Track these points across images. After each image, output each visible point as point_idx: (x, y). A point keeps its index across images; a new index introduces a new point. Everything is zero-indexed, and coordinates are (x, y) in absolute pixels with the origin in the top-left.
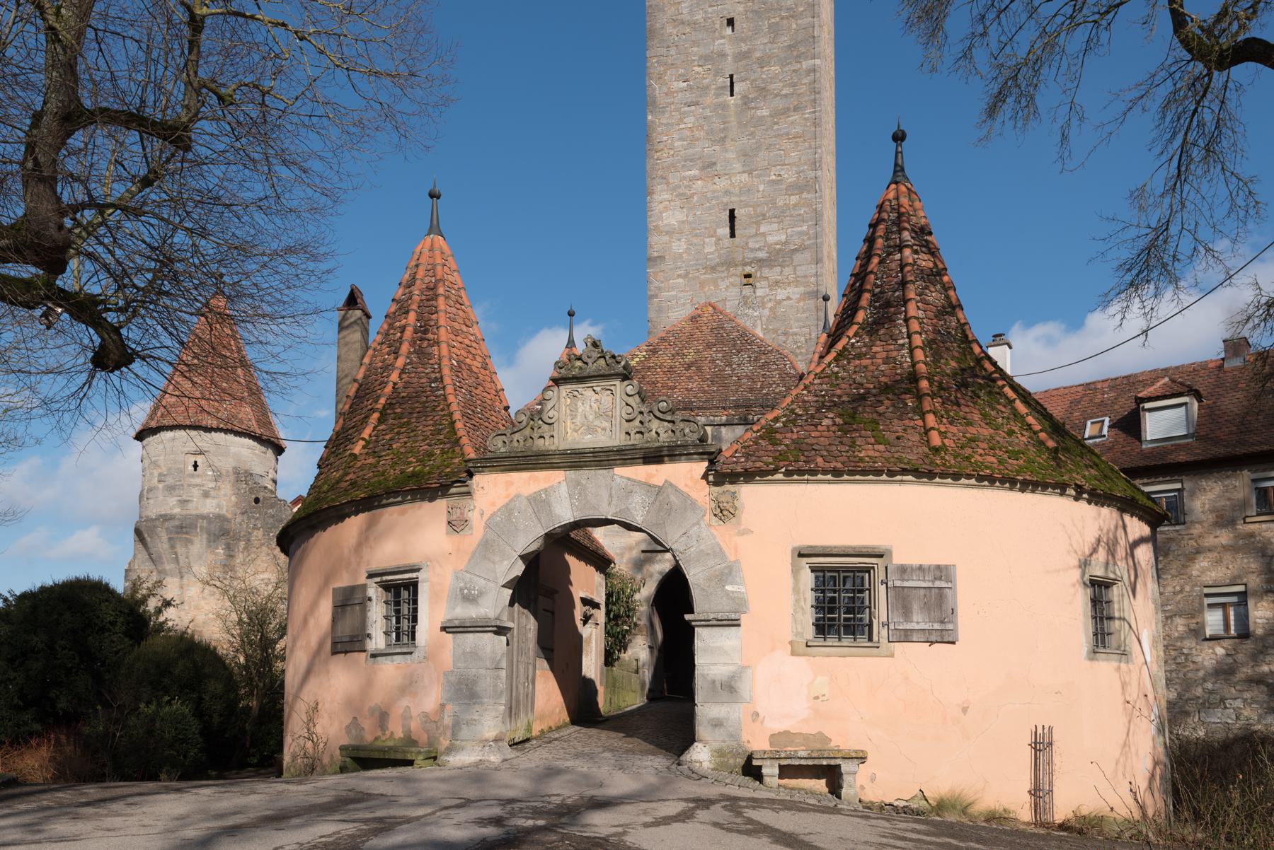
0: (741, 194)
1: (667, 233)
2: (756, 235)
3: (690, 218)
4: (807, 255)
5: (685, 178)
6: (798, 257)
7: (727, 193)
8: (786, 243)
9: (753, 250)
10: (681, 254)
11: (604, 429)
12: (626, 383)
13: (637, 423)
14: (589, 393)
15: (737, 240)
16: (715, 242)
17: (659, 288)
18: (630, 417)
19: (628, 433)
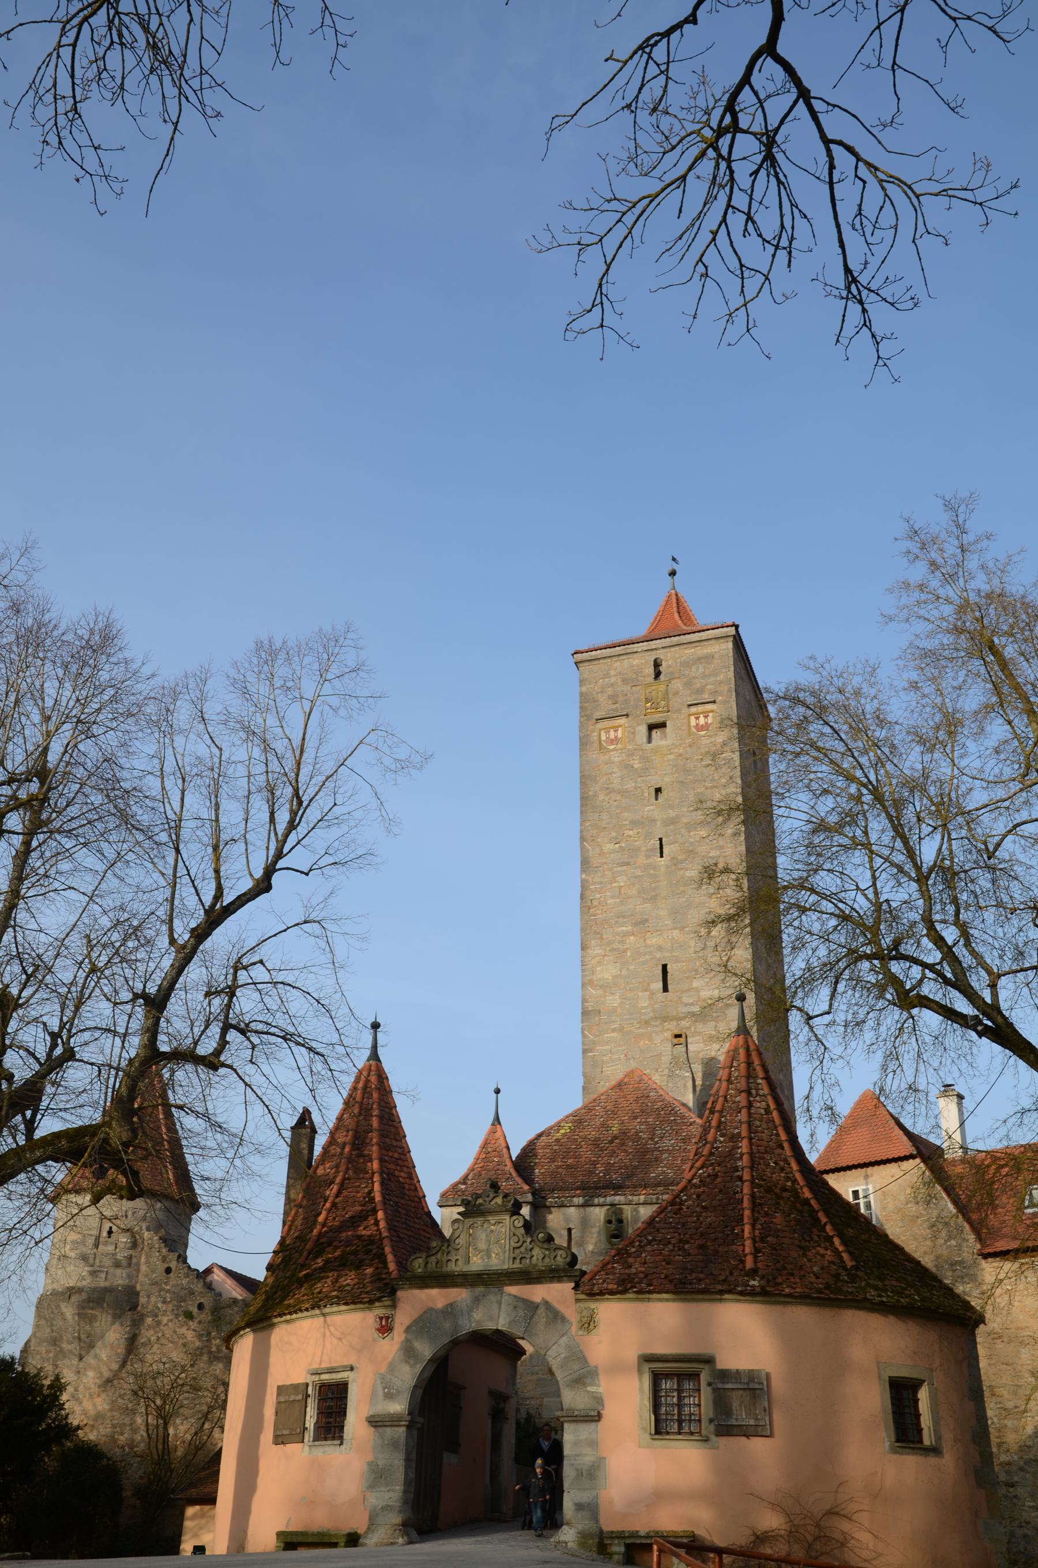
1: (601, 987)
2: (688, 991)
3: (624, 972)
5: (618, 934)
7: (660, 948)
9: (686, 1005)
10: (615, 1010)
12: (514, 1217)
13: (522, 1249)
16: (648, 998)
17: (594, 1042)
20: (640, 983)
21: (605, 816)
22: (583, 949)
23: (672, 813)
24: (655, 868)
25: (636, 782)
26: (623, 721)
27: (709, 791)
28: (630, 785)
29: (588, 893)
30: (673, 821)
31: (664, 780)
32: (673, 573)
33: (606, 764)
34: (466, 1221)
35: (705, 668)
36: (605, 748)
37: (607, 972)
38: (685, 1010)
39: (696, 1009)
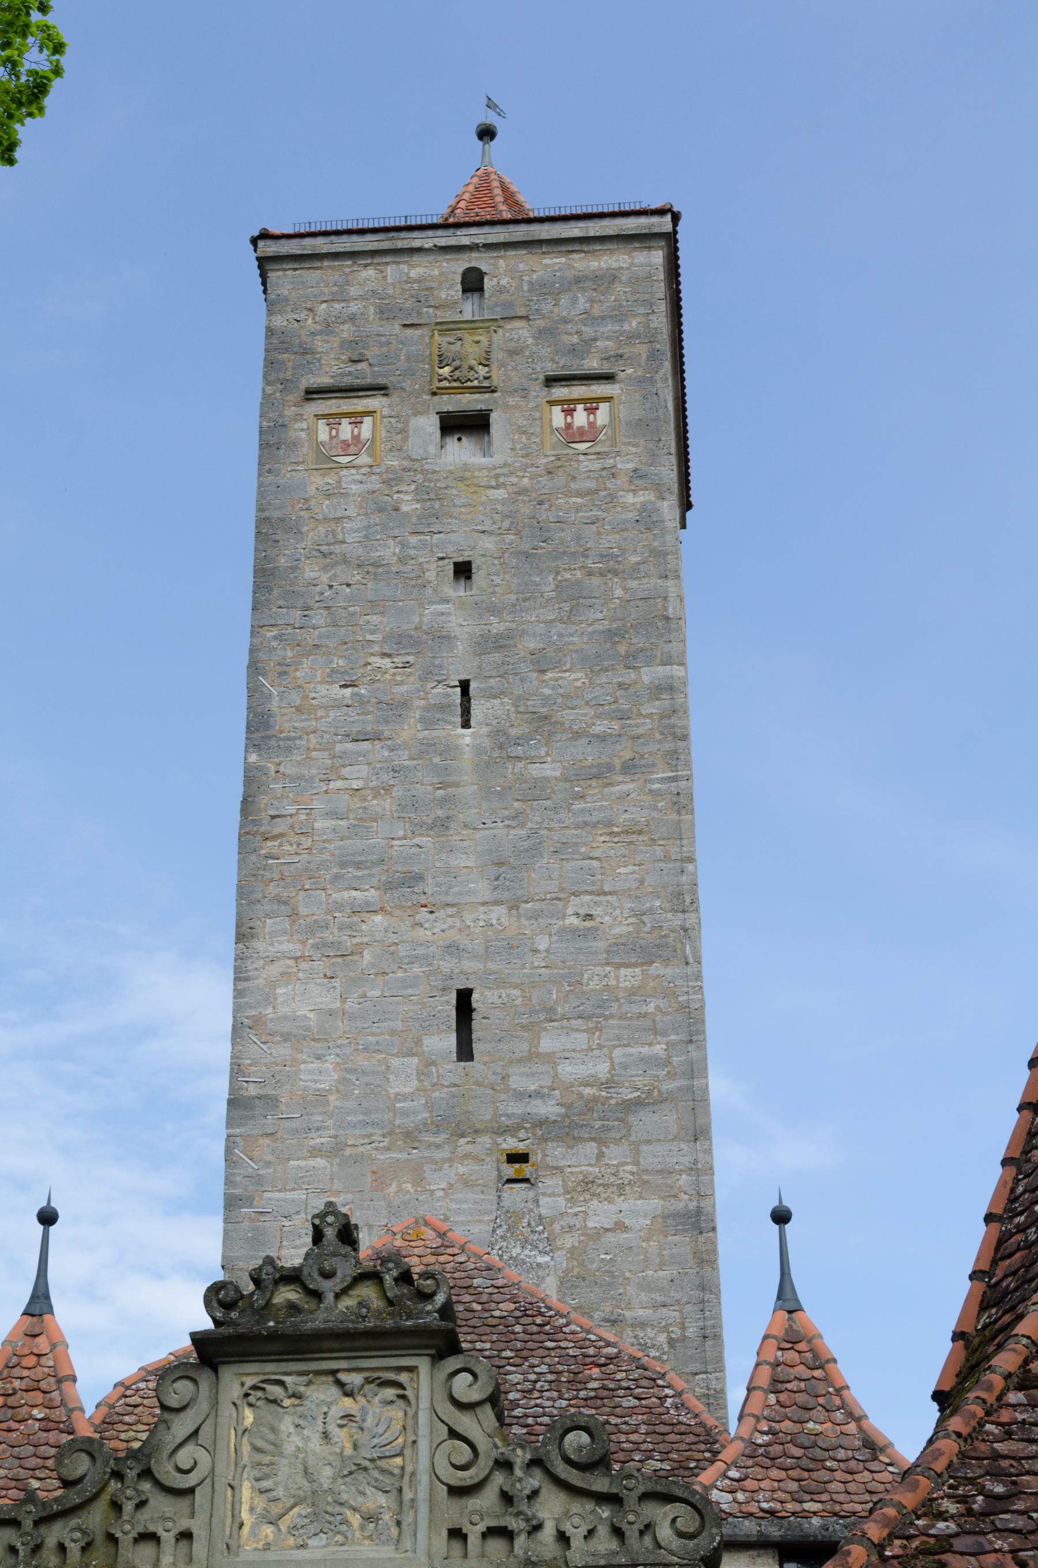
0: (488, 954)
1: (286, 1037)
4: (668, 1118)
5: (339, 906)
6: (644, 1122)
7: (452, 949)
8: (609, 1084)
10: (322, 1095)
11: (370, 1518)
12: (453, 1363)
14: (322, 1394)
15: (475, 1067)
16: (417, 1069)
17: (258, 1180)
18: (468, 1477)
19: (457, 1534)
20: (393, 1033)
21: (319, 618)
22: (241, 937)
23: (497, 626)
24: (449, 751)
25: (404, 545)
26: (374, 402)
27: (596, 581)
28: (389, 551)
29: (263, 800)
30: (500, 643)
31: (482, 550)
32: (486, 133)
33: (328, 496)
34: (227, 1373)
35: (592, 301)
36: (329, 459)
37: (304, 1000)
38: (517, 1109)
39: (548, 1109)
